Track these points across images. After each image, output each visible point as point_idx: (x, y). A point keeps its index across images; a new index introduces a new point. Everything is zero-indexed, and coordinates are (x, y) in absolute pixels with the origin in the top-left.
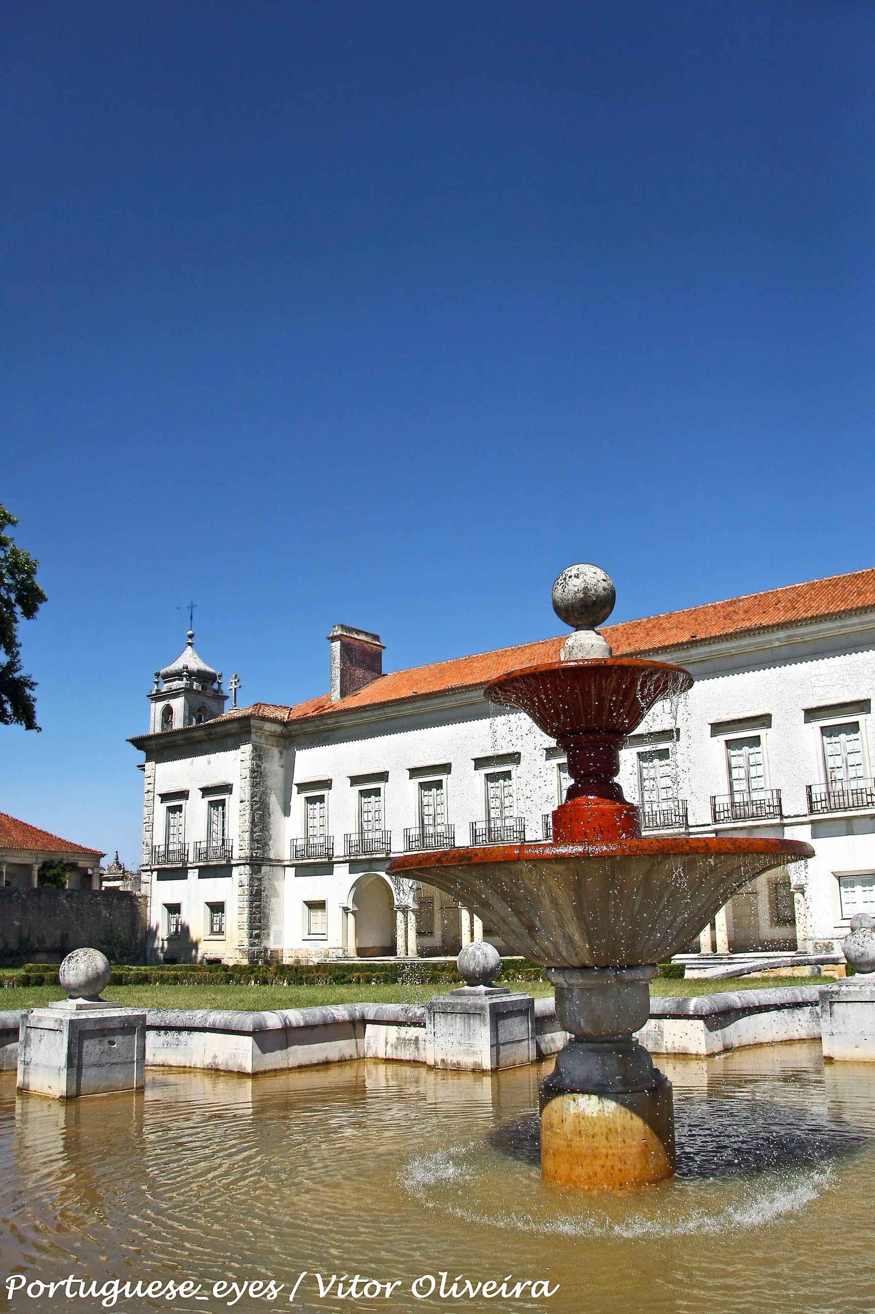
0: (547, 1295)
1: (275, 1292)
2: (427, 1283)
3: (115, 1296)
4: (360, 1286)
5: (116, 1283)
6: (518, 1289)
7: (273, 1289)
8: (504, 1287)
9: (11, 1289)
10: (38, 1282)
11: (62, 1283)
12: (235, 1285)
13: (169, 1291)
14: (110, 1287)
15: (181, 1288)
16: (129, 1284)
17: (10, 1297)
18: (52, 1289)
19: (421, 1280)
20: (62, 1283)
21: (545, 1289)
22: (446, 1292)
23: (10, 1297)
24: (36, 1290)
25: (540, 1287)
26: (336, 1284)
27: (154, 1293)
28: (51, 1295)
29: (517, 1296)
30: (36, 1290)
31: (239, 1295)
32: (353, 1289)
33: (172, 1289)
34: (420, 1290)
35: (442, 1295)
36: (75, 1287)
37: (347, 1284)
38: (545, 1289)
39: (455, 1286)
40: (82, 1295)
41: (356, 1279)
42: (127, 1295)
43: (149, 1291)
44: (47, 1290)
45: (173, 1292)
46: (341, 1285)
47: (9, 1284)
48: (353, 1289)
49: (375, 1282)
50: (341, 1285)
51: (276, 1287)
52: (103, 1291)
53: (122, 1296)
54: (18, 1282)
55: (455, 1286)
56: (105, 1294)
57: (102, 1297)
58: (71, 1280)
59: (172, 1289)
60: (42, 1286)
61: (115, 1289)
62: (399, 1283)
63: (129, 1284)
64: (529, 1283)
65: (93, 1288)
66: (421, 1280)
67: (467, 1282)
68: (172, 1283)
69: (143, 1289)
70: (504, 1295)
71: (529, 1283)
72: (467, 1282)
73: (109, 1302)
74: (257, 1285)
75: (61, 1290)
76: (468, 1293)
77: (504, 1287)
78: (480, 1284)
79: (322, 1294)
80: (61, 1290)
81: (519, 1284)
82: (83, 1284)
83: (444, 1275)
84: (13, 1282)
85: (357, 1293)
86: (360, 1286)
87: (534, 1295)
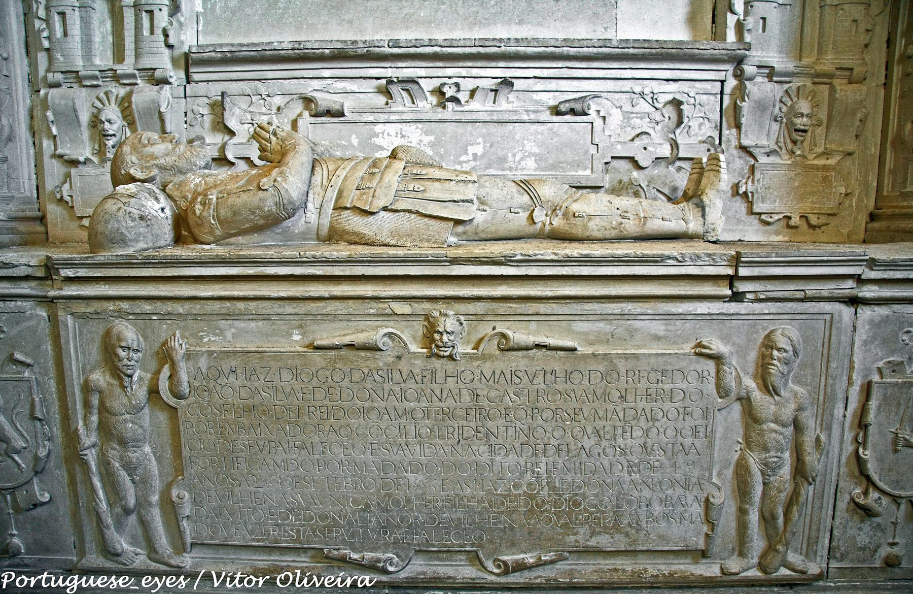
1: (184, 584)
4: (241, 580)
5: (76, 577)
9: (5, 581)
10: (23, 577)
11: (40, 577)
12: (157, 579)
13: (112, 583)
15: (120, 581)
16: (85, 578)
17: (4, 587)
18: (33, 581)
19: (283, 575)
20: (40, 577)
23: (4, 587)
24: (22, 581)
26: (224, 580)
28: (32, 586)
29: (348, 586)
30: (22, 581)
31: (160, 585)
32: (237, 581)
34: (282, 582)
35: (297, 585)
36: (48, 580)
38: (367, 582)
39: (306, 579)
40: (53, 585)
43: (99, 582)
44: (29, 582)
45: (115, 583)
46: (228, 579)
47: (3, 578)
48: (237, 581)
50: (228, 579)
51: (185, 580)
52: (67, 583)
53: (80, 586)
54: (10, 577)
55: (306, 579)
57: (67, 587)
58: (45, 575)
60: (26, 579)
61: (75, 581)
62: (268, 577)
63: (85, 578)
64: (356, 577)
66: (283, 575)
70: (339, 585)
76: (314, 583)
77: (339, 580)
79: (216, 585)
80: (40, 581)
82: (54, 578)
83: (299, 572)
84: (6, 577)
85: (240, 583)
86: (241, 580)
87: (359, 585)
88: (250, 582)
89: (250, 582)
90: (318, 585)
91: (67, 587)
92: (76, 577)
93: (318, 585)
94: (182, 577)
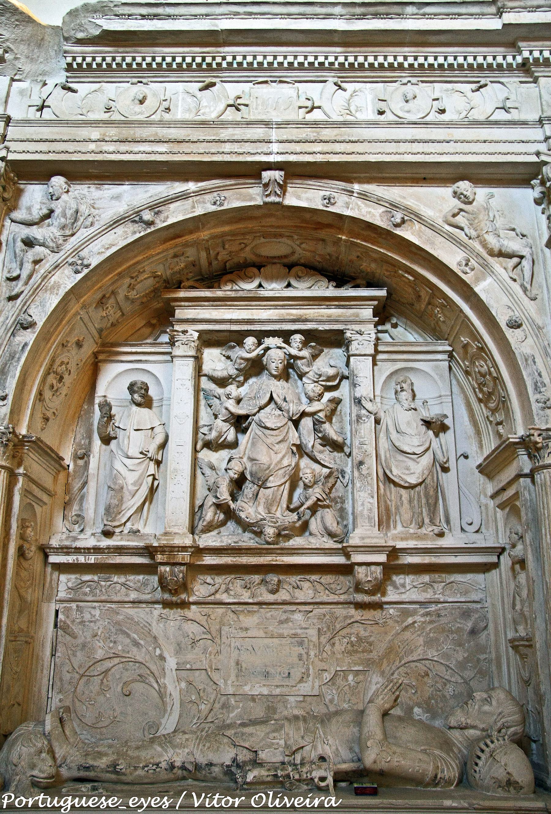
1: (167, 804)
2: (261, 797)
3: (69, 807)
4: (219, 801)
5: (70, 798)
7: (166, 802)
8: (308, 800)
9: (5, 802)
11: (37, 798)
12: (143, 800)
14: (67, 800)
15: (110, 801)
17: (4, 807)
20: (37, 798)
21: (333, 802)
23: (4, 807)
24: (20, 802)
27: (93, 804)
28: (30, 806)
29: (316, 806)
30: (20, 802)
31: (145, 805)
32: (215, 802)
33: (104, 802)
37: (212, 799)
38: (333, 802)
39: (278, 800)
40: (49, 806)
41: (217, 796)
42: (77, 806)
43: (90, 803)
44: (27, 803)
45: (105, 804)
46: (208, 799)
48: (215, 802)
49: (228, 798)
50: (208, 799)
51: (168, 801)
52: (62, 803)
53: (73, 806)
54: (9, 797)
55: (278, 800)
56: (63, 805)
57: (61, 807)
59: (104, 802)
63: (77, 799)
64: (323, 798)
67: (285, 797)
68: (104, 798)
71: (323, 798)
72: (285, 797)
74: (156, 800)
76: (285, 804)
77: (308, 800)
78: (293, 799)
81: (317, 799)
82: (49, 799)
83: (271, 793)
84: (6, 797)
88: (227, 802)
89: (227, 802)
90: (288, 805)
91: (61, 807)
92: (70, 798)
93: (288, 805)
94: (166, 798)
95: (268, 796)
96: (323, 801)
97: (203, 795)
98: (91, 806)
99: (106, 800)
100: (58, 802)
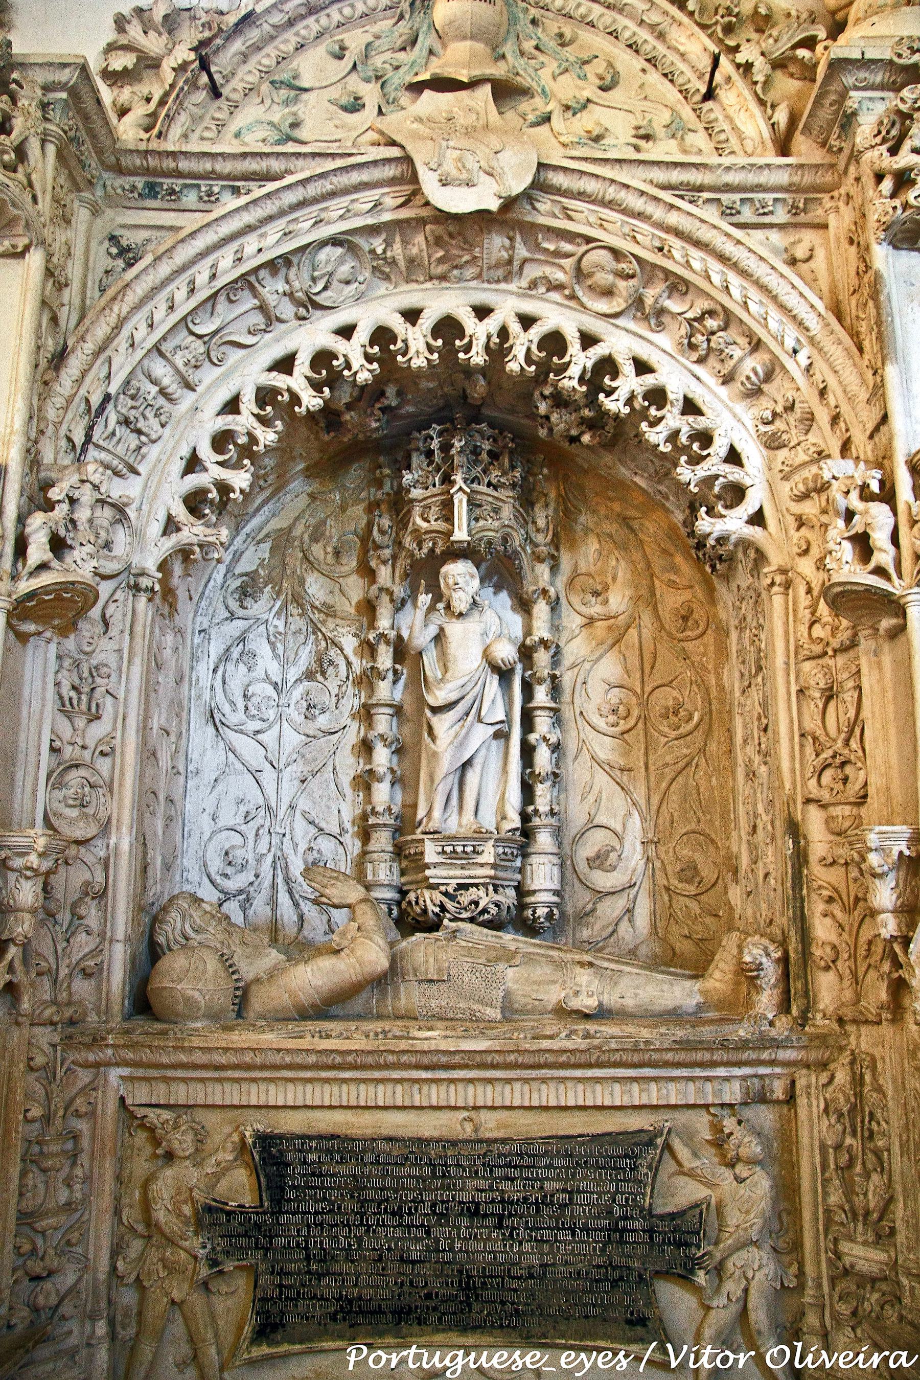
0: (905, 1365)
2: (782, 1352)
3: (459, 1367)
5: (461, 1353)
6: (876, 1359)
8: (861, 1357)
9: (352, 1359)
13: (514, 1362)
15: (528, 1359)
17: (351, 1368)
19: (775, 1350)
20: (405, 1353)
21: (903, 1360)
22: (695, 1362)
23: (351, 1368)
24: (377, 1360)
25: (899, 1356)
30: (377, 1360)
31: (588, 1366)
35: (797, 1366)
36: (418, 1357)
38: (903, 1360)
40: (425, 1366)
41: (708, 1351)
42: (472, 1366)
43: (495, 1361)
45: (520, 1363)
46: (692, 1356)
49: (727, 1353)
52: (447, 1362)
53: (465, 1366)
58: (414, 1349)
60: (384, 1357)
63: (473, 1354)
65: (436, 1359)
66: (775, 1350)
68: (518, 1353)
69: (489, 1359)
70: (861, 1366)
73: (453, 1373)
75: (403, 1361)
77: (861, 1357)
79: (674, 1364)
80: (403, 1361)
87: (892, 1366)
88: (725, 1360)
89: (725, 1360)
90: (828, 1365)
93: (828, 1365)
95: (793, 1350)
96: (886, 1358)
97: (685, 1347)
98: (497, 1366)
99: (521, 1357)
100: (441, 1361)
